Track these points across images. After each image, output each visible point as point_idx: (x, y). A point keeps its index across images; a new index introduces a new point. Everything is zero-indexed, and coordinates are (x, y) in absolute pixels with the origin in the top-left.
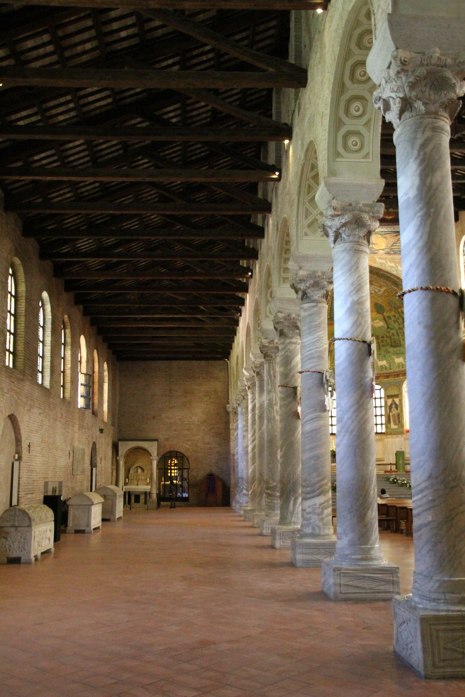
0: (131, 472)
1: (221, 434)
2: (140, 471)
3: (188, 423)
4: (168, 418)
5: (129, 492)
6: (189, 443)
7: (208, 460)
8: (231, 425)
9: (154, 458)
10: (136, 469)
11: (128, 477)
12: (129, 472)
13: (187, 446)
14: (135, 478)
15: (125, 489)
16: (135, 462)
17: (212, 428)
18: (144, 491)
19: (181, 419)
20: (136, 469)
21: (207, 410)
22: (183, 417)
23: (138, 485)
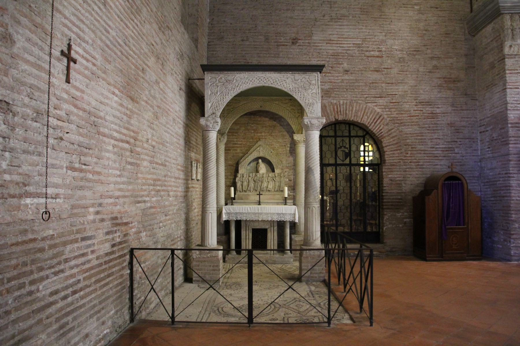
0: (241, 171)
1: (455, 81)
2: (263, 168)
3: (377, 54)
4: (329, 41)
5: (238, 223)
6: (381, 101)
7: (430, 144)
8: (508, 44)
9: (315, 122)
10: (255, 162)
11: (234, 184)
12: (237, 171)
13: (379, 110)
14: (252, 185)
15: (228, 214)
16: (250, 147)
17: (436, 67)
18: (276, 218)
19: (358, 46)
20: (255, 162)
21: (421, 25)
22: (364, 40)
23: (259, 203)
